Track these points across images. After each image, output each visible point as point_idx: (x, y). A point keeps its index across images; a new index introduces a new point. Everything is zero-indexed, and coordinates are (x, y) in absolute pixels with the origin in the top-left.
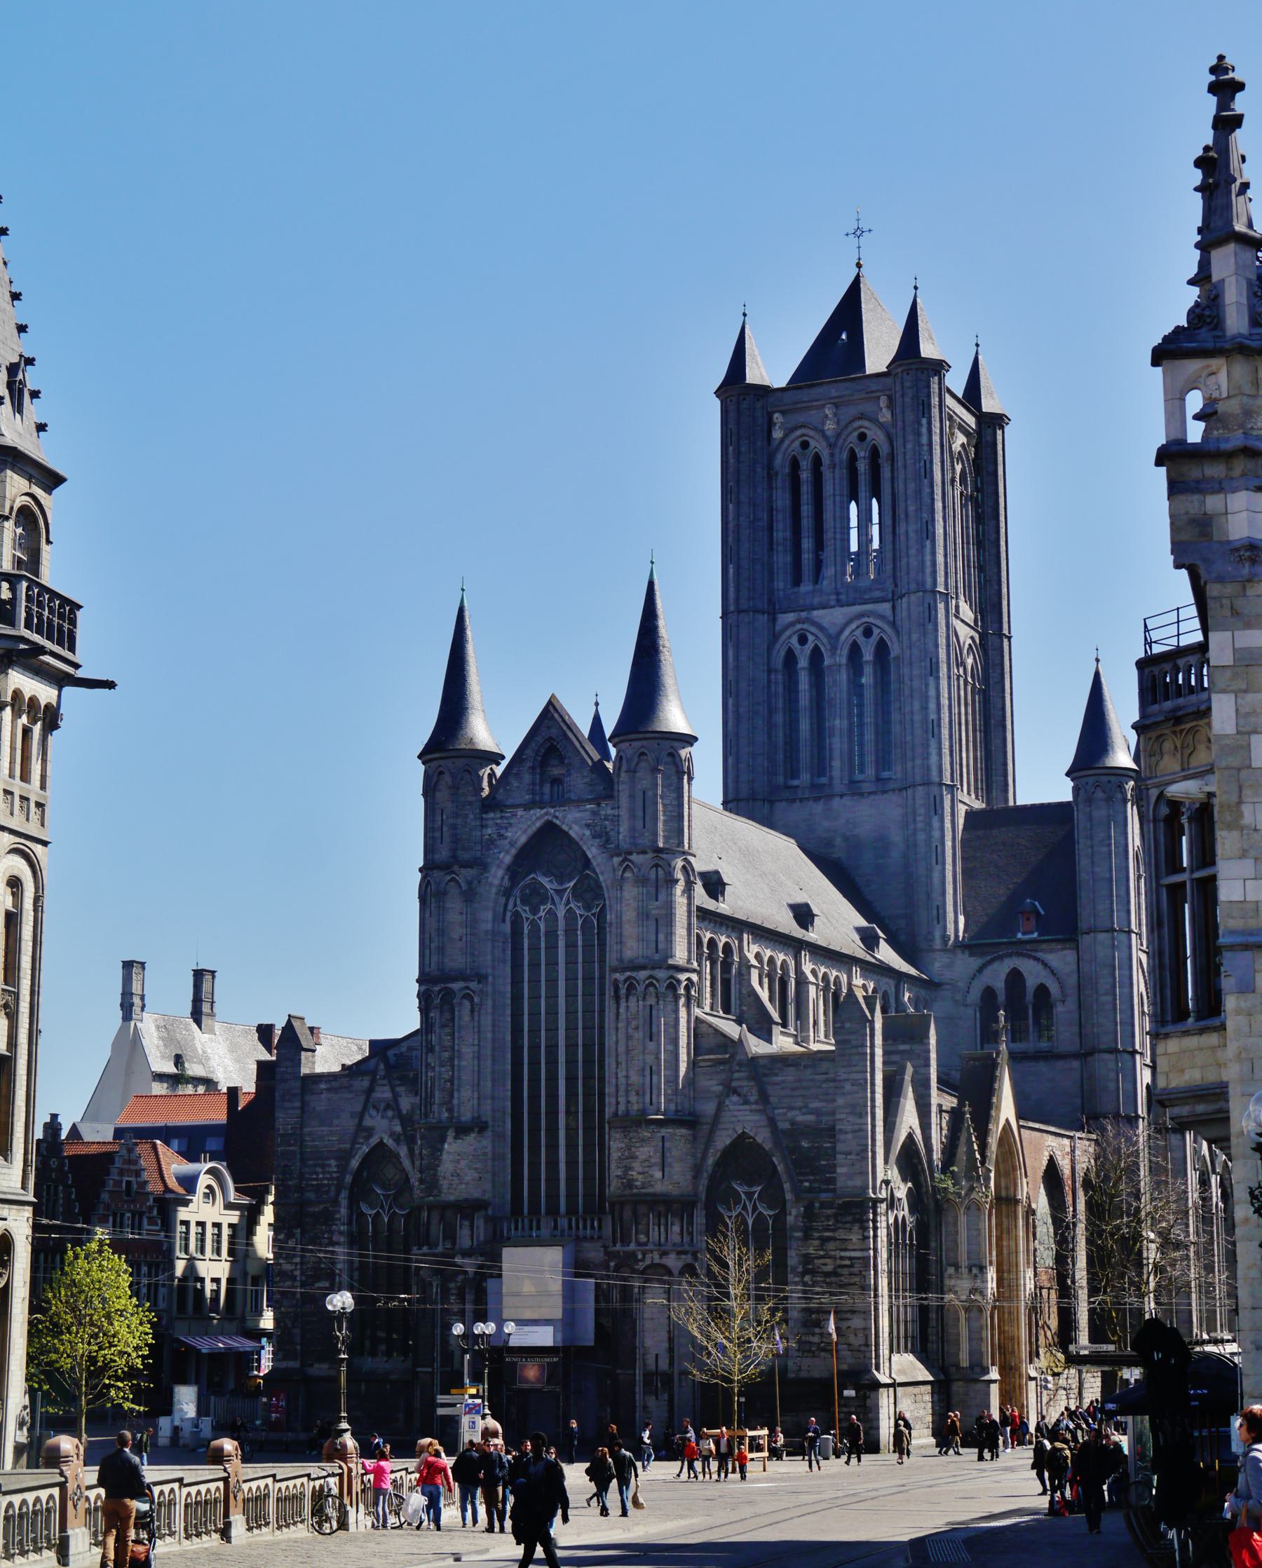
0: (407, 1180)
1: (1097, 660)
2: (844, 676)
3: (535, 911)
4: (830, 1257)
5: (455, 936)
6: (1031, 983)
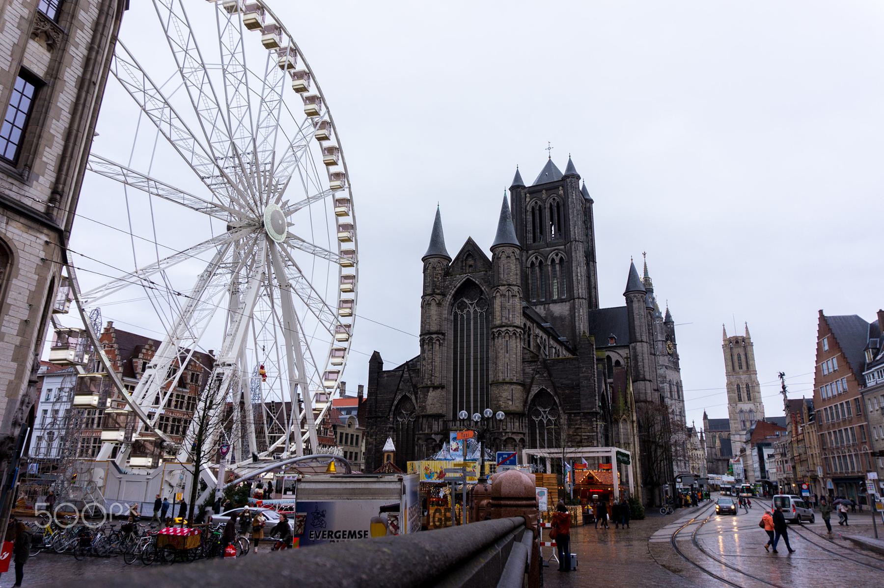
0: (414, 408)
1: (632, 260)
2: (550, 269)
3: (462, 311)
4: (579, 435)
5: (434, 319)
6: (614, 360)
